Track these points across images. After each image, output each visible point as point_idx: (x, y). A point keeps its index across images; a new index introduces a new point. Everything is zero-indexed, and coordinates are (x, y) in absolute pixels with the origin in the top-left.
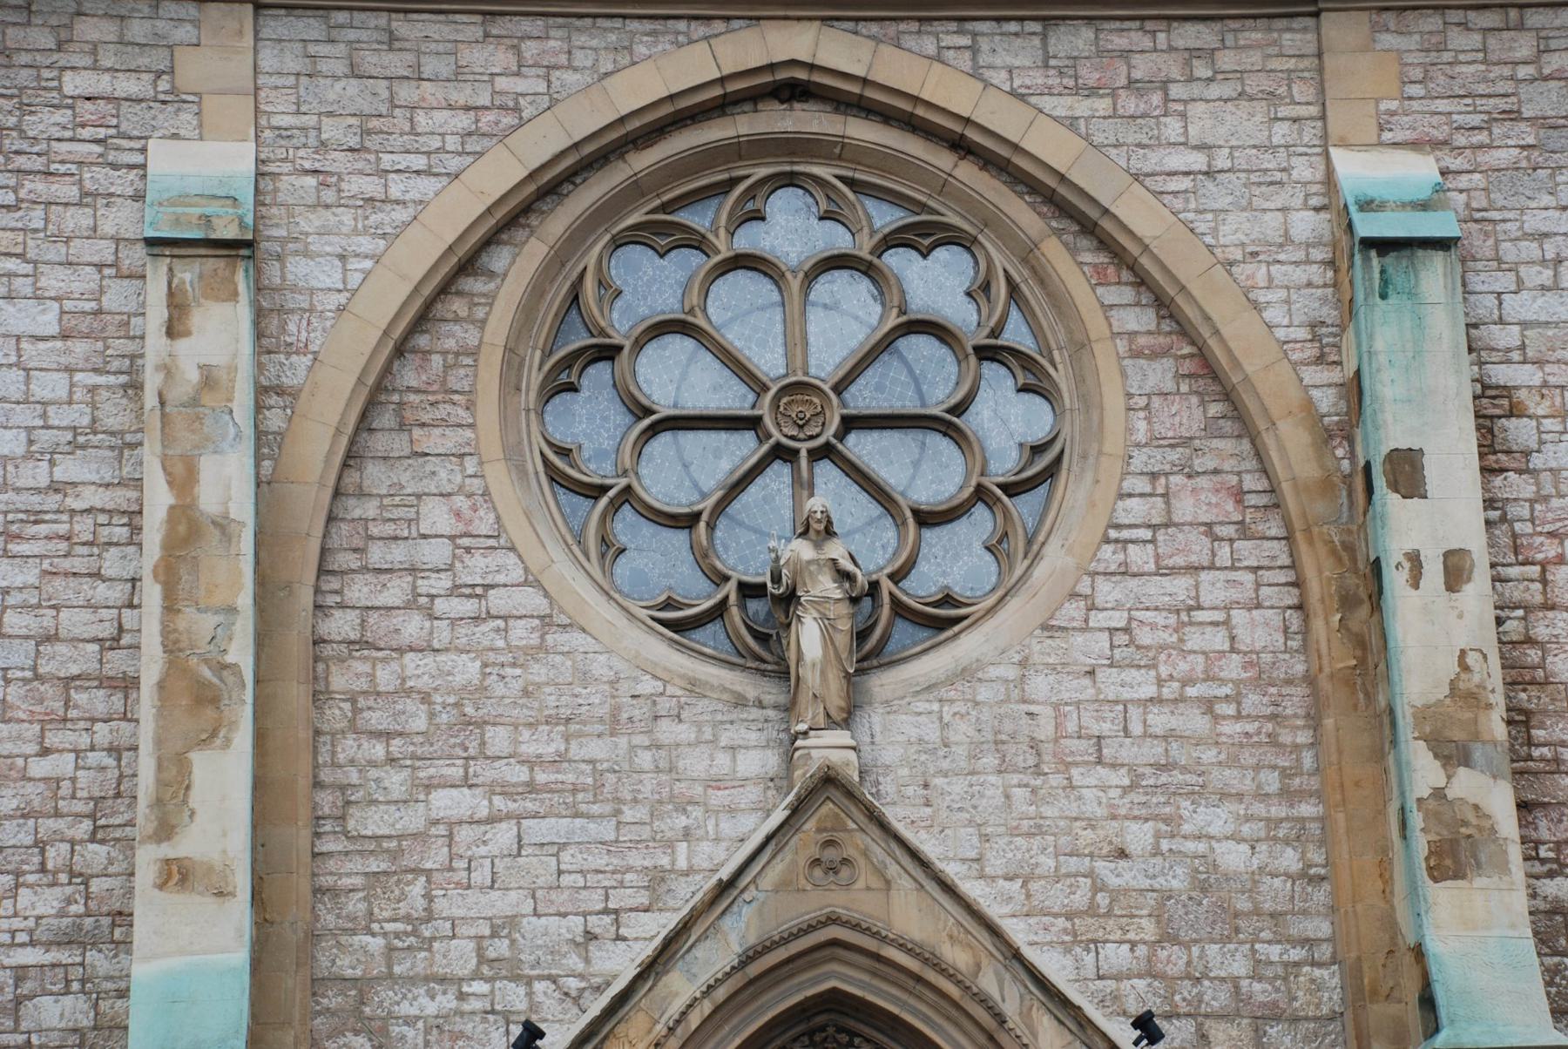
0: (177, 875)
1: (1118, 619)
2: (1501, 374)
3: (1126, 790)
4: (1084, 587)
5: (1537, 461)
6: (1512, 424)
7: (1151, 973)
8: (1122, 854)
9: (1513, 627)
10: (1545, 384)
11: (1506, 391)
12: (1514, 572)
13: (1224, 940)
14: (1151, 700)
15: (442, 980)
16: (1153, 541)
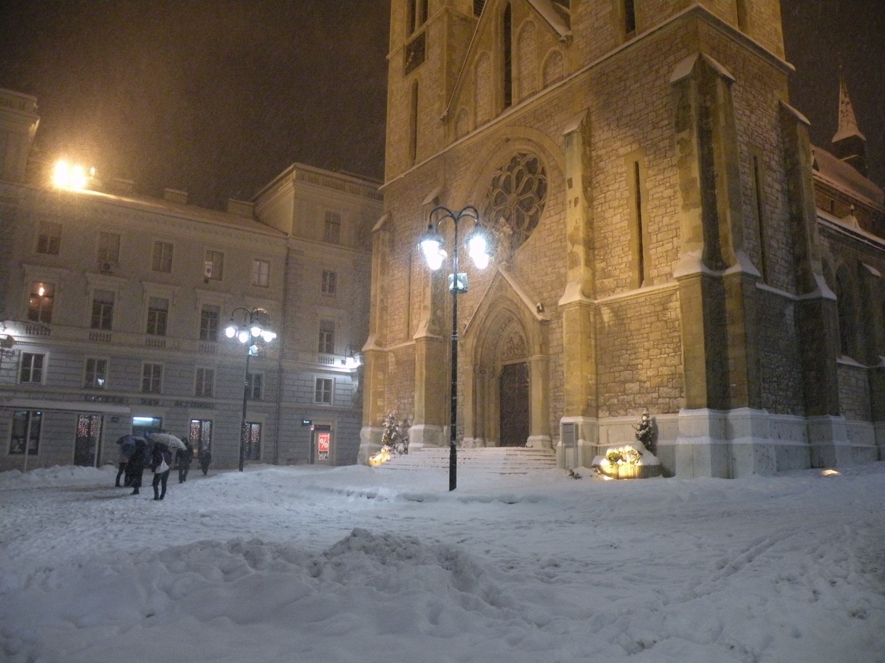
0: (425, 308)
1: (548, 226)
2: (600, 153)
3: (549, 261)
4: (544, 222)
5: (605, 170)
6: (601, 164)
7: (550, 297)
8: (547, 274)
9: (599, 210)
10: (607, 152)
11: (601, 156)
12: (600, 197)
13: (560, 288)
14: (553, 242)
15: (465, 317)
16: (554, 209)
